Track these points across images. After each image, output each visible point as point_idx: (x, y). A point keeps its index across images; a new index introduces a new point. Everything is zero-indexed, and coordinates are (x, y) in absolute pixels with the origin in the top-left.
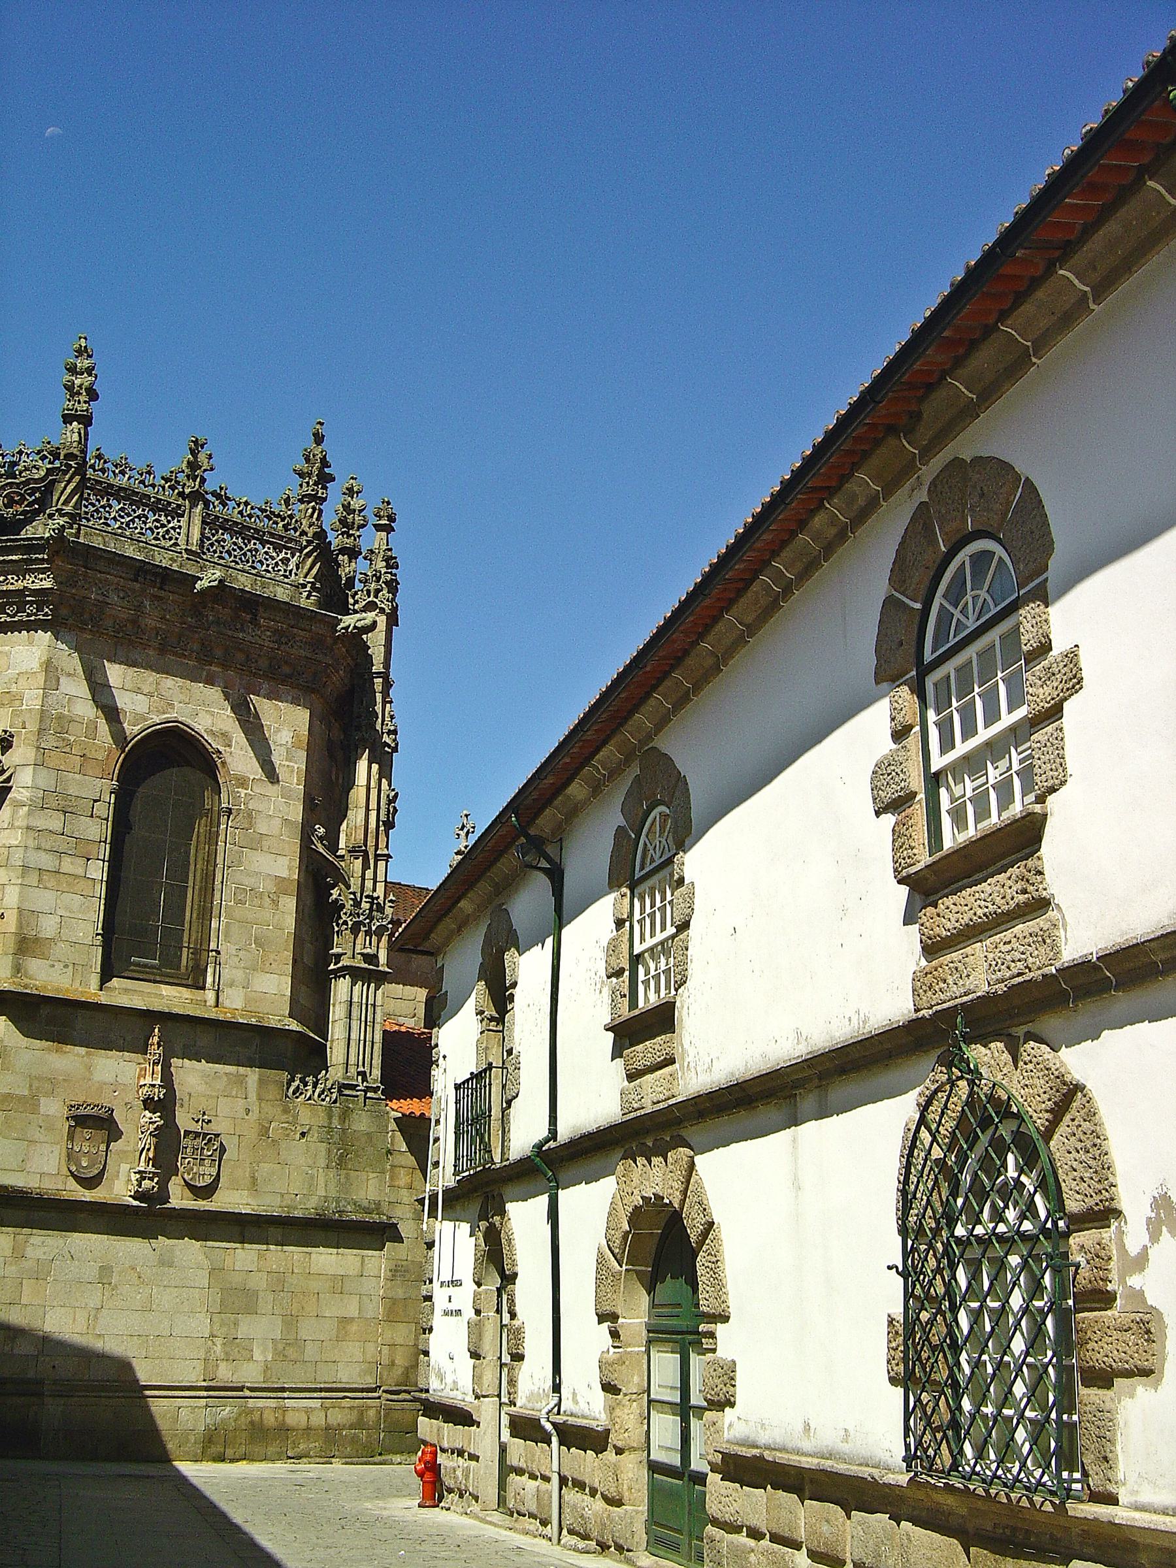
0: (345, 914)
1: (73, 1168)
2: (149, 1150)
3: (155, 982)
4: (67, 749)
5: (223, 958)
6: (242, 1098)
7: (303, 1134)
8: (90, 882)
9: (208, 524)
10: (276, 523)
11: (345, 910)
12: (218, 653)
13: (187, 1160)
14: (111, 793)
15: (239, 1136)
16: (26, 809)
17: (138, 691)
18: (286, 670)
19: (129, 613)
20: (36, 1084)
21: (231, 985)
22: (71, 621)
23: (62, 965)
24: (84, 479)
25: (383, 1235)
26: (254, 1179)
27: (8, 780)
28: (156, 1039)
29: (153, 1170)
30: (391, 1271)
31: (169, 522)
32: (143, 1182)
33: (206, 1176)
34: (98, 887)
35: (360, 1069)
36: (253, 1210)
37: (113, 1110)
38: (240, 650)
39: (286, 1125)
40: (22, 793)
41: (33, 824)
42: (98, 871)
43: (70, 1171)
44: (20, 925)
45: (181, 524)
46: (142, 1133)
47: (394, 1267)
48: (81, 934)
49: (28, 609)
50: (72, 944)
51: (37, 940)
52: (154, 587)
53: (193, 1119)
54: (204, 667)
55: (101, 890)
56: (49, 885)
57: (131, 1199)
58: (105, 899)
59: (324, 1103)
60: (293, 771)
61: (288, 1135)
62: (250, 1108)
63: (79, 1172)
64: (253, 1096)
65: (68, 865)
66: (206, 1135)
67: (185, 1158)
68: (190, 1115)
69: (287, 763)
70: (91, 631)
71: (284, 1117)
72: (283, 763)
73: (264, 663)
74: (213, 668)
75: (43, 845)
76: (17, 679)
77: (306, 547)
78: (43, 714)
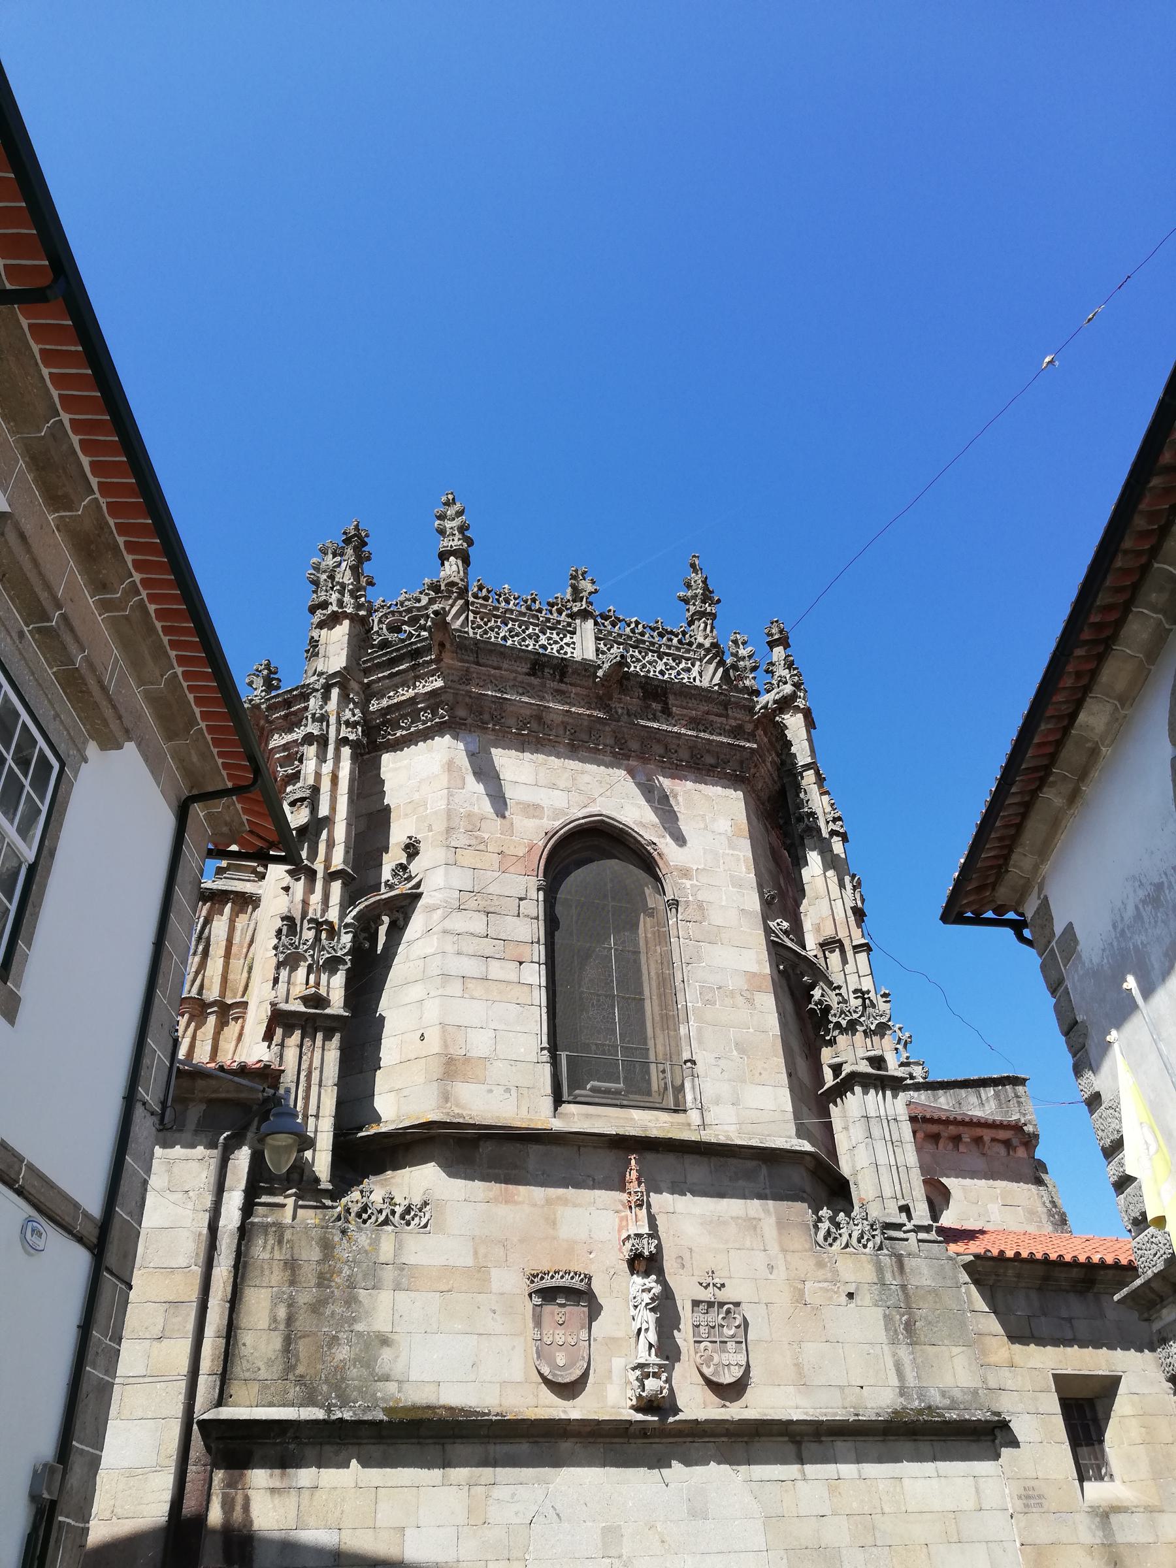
0: (835, 1015)
1: (546, 1371)
2: (647, 1330)
3: (622, 1106)
4: (482, 847)
5: (700, 1068)
6: (760, 1250)
7: (850, 1295)
8: (527, 988)
9: (601, 639)
10: (670, 640)
11: (832, 1012)
13: (703, 1345)
14: (539, 890)
16: (439, 912)
17: (554, 786)
18: (710, 760)
19: (531, 709)
20: (482, 1250)
21: (717, 1101)
22: (469, 721)
23: (501, 1089)
24: (467, 603)
25: (993, 1441)
27: (418, 885)
28: (634, 1174)
29: (658, 1361)
30: (1020, 1497)
31: (561, 639)
32: (646, 1382)
33: (732, 1367)
34: (536, 992)
35: (901, 1203)
36: (806, 1414)
37: (590, 1278)
38: (659, 741)
39: (826, 1284)
40: (434, 896)
41: (448, 924)
42: (535, 975)
43: (541, 1375)
44: (446, 1046)
45: (574, 640)
46: (636, 1307)
47: (1022, 1492)
48: (522, 1050)
49: (423, 716)
50: (513, 1063)
51: (466, 1059)
52: (553, 681)
53: (701, 1284)
54: (621, 761)
55: (541, 997)
56: (476, 994)
57: (632, 1412)
58: (547, 1007)
59: (867, 1250)
60: (739, 860)
61: (831, 1298)
62: (772, 1263)
63: (554, 1375)
64: (774, 1248)
65: (497, 970)
66: (721, 1305)
67: (700, 1342)
68: (696, 1279)
69: (731, 852)
70: (493, 730)
71: (821, 1274)
72: (727, 851)
73: (684, 754)
74: (630, 762)
75: (465, 949)
76: (419, 787)
77: (705, 656)
78: (449, 814)
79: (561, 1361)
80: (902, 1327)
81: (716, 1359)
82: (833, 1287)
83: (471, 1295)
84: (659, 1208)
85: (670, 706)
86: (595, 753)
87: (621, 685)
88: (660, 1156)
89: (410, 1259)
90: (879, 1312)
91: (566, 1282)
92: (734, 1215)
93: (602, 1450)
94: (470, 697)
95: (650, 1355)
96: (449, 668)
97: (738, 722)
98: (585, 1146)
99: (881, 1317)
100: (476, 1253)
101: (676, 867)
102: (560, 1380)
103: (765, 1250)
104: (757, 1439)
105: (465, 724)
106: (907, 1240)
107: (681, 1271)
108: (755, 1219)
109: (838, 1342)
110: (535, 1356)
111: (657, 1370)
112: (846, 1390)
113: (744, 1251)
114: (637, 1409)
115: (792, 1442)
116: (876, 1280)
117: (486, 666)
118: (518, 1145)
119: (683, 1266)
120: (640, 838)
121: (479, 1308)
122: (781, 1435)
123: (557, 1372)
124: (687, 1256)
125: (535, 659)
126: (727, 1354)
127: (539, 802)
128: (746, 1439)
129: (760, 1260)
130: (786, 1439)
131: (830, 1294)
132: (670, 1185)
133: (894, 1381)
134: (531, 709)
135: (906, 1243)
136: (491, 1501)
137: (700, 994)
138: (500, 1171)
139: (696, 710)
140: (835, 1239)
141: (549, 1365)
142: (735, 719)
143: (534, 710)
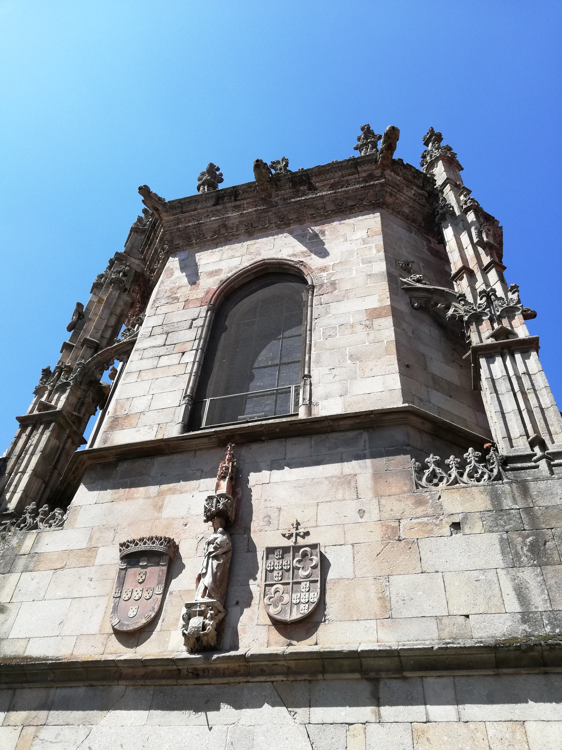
5: (314, 380)
12: (293, 216)
18: (350, 203)
26: (384, 600)
38: (308, 207)
39: (425, 520)
51: (127, 416)
62: (364, 508)
65: (164, 361)
67: (272, 585)
68: (280, 532)
70: (196, 244)
71: (420, 511)
80: (525, 549)
81: (286, 598)
82: (435, 521)
85: (314, 184)
86: (266, 231)
87: (277, 185)
88: (265, 444)
89: (41, 549)
90: (495, 537)
93: (151, 692)
94: (180, 231)
96: (167, 222)
97: (367, 173)
98: (200, 450)
99: (497, 542)
100: (91, 539)
101: (317, 269)
104: (320, 677)
105: (179, 248)
106: (537, 467)
107: (267, 528)
109: (437, 572)
112: (445, 621)
115: (369, 680)
116: (490, 507)
117: (188, 212)
120: (290, 262)
121: (80, 578)
122: (352, 671)
124: (274, 515)
125: (217, 195)
127: (221, 267)
128: (306, 677)
129: (352, 507)
130: (357, 676)
131: (429, 527)
133: (513, 605)
134: (218, 222)
135: (536, 470)
136: (37, 741)
137: (323, 333)
139: (333, 178)
140: (441, 479)
142: (365, 171)
143: (220, 222)
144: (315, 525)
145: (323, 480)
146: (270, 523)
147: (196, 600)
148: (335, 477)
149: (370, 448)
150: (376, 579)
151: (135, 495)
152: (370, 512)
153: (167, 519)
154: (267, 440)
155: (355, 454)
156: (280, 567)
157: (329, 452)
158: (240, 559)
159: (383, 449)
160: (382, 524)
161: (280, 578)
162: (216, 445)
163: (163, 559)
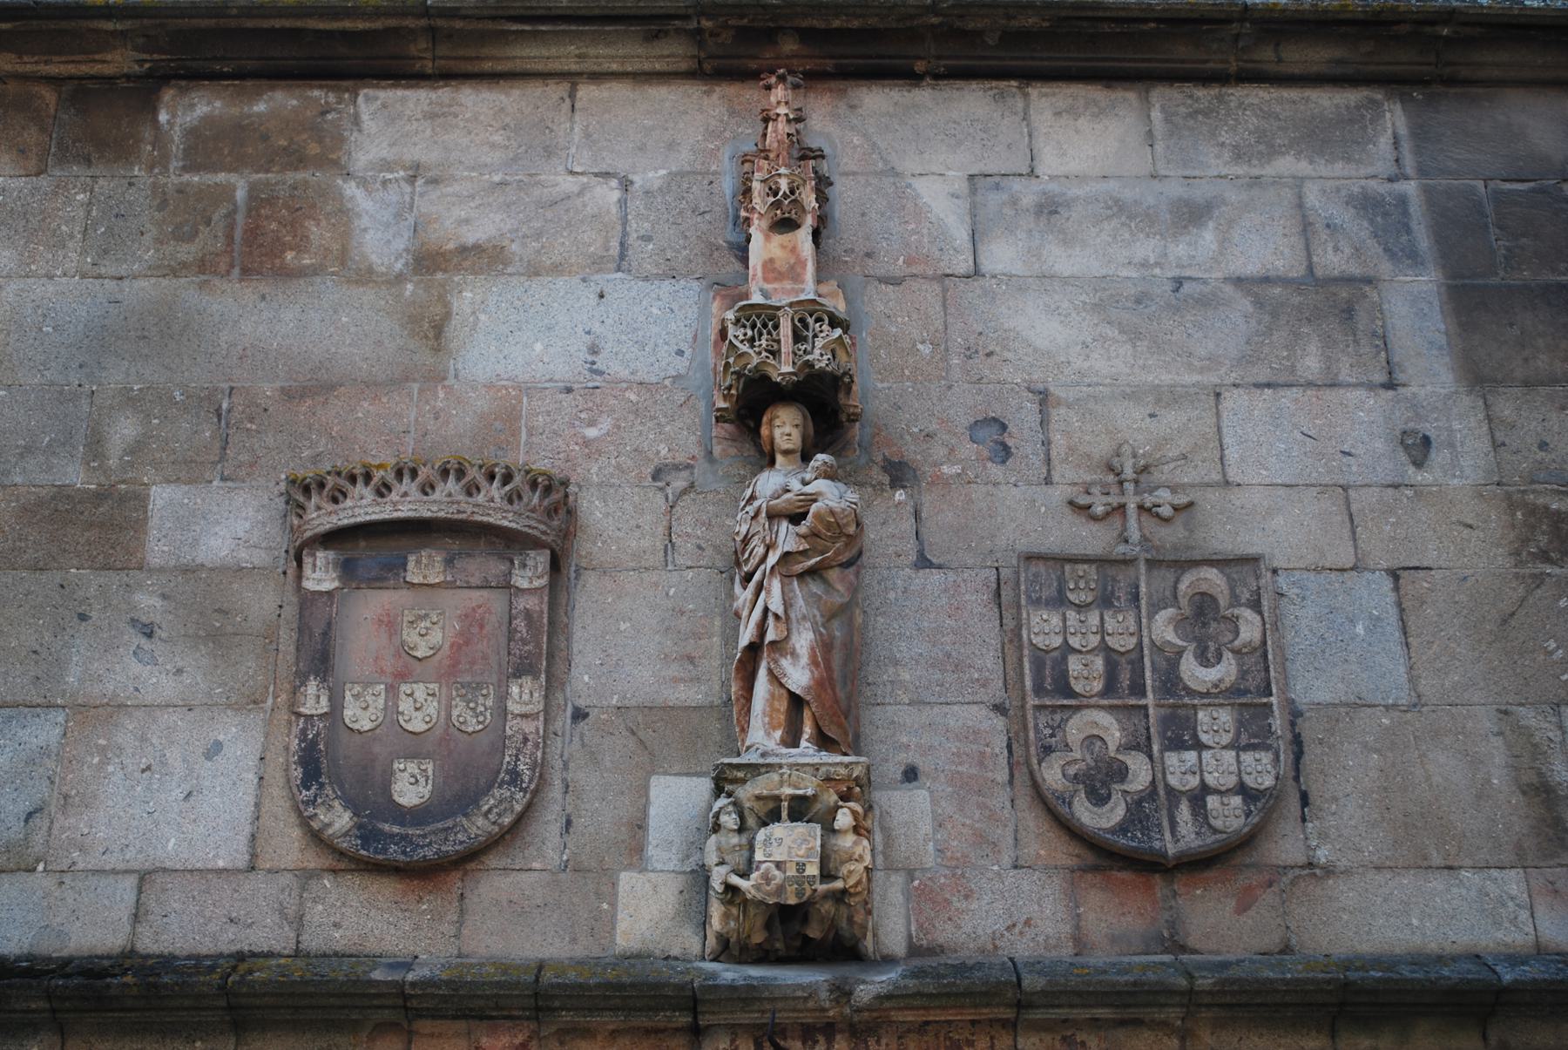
1: (339, 820)
6: (1371, 387)
13: (1075, 729)
15: (1394, 574)
33: (1212, 802)
46: (748, 578)
68: (1059, 494)
79: (410, 789)
83: (58, 577)
84: (908, 262)
88: (923, 95)
91: (444, 502)
92: (1252, 269)
95: (792, 740)
102: (394, 852)
103: (1390, 385)
107: (995, 471)
108: (1348, 280)
110: (297, 773)
111: (810, 792)
113: (1294, 392)
114: (726, 950)
118: (316, 93)
119: (1004, 453)
123: (386, 827)
124: (1022, 419)
126: (1191, 756)
132: (962, 186)
138: (233, 177)
141: (351, 804)
144: (1216, 476)
145: (1229, 289)
146: (1006, 449)
147: (763, 755)
148: (1284, 281)
149: (1422, 172)
150: (1506, 713)
151: (289, 255)
152: (1451, 445)
153: (489, 386)
154: (937, 77)
155: (1356, 190)
156: (1094, 640)
157: (1240, 170)
158: (892, 595)
159: (1480, 184)
160: (1508, 496)
161: (1098, 686)
162: (683, 66)
163: (524, 566)
